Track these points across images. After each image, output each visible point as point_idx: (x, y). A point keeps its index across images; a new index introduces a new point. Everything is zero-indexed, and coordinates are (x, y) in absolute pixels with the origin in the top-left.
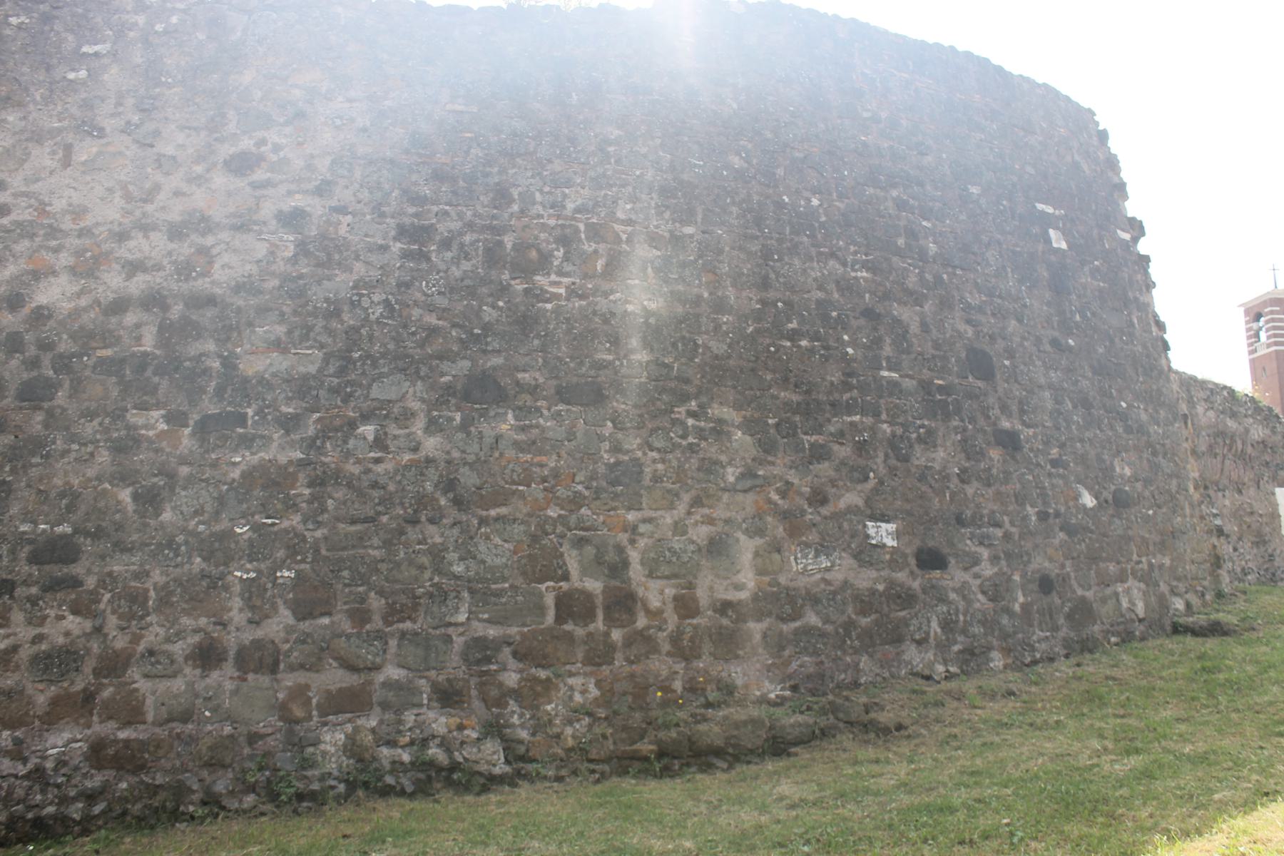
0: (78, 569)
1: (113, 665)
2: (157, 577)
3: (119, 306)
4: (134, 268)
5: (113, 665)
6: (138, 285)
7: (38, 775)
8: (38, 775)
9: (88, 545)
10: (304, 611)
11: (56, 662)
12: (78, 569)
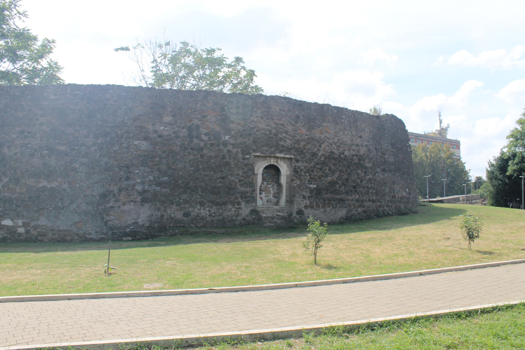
0: (357, 189)
1: (362, 201)
2: (364, 191)
3: (353, 156)
4: (354, 150)
5: (362, 201)
6: (354, 153)
7: (359, 213)
8: (359, 213)
9: (358, 187)
10: (376, 196)
11: (357, 200)
12: (357, 189)
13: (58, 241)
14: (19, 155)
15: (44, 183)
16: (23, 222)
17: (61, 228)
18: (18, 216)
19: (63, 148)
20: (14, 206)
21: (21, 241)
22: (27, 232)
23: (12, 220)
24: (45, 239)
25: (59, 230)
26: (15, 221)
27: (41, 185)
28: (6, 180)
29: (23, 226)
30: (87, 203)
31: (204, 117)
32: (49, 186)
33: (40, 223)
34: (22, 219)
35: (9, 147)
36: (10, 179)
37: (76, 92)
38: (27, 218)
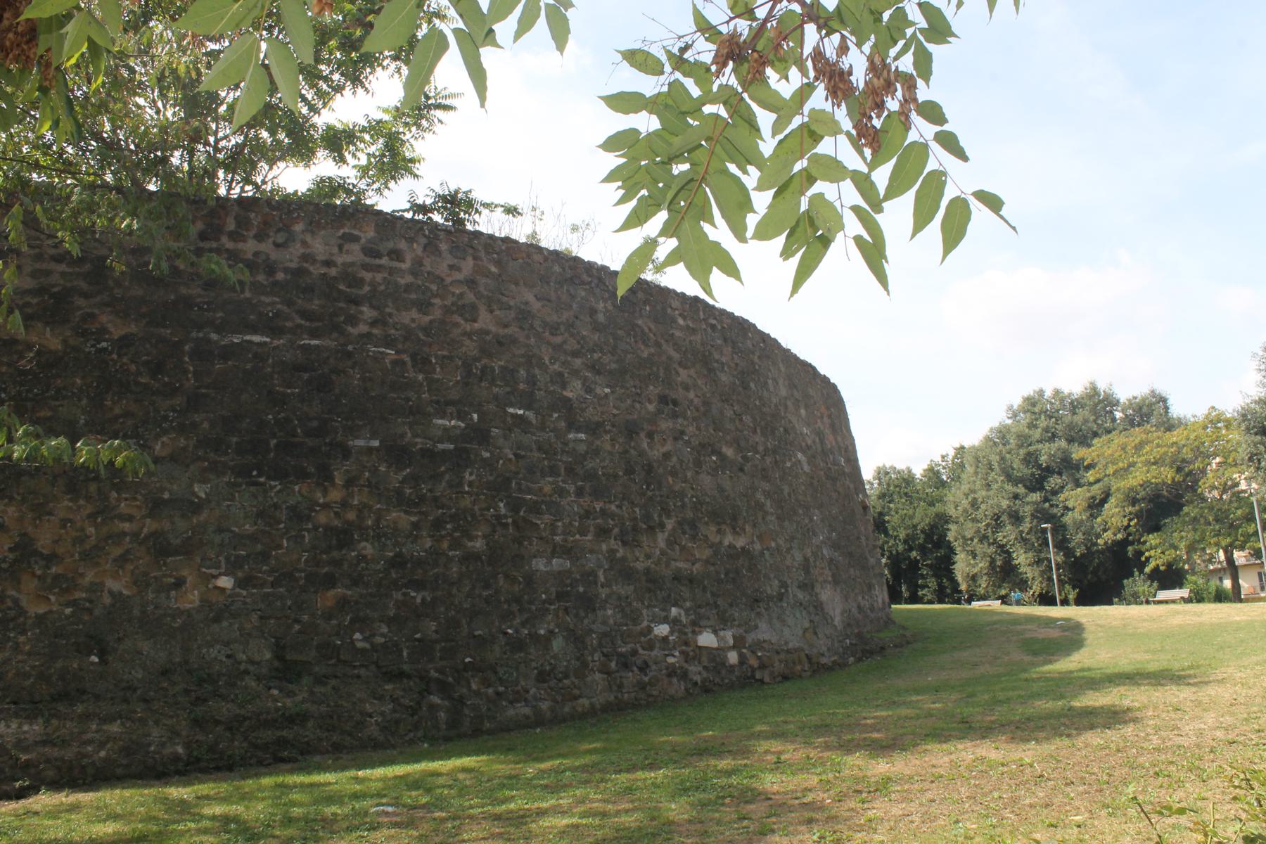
13: (786, 678)
14: (674, 459)
15: (728, 539)
16: (734, 637)
17: (791, 645)
18: (724, 621)
19: (729, 452)
20: (709, 595)
21: (731, 687)
22: (743, 660)
23: (715, 632)
24: (767, 679)
25: (788, 651)
26: (721, 633)
27: (726, 543)
28: (670, 524)
29: (734, 647)
30: (799, 587)
31: (822, 417)
32: (740, 543)
33: (762, 636)
34: (732, 627)
35: (650, 435)
36: (680, 524)
37: (714, 322)
38: (739, 626)
